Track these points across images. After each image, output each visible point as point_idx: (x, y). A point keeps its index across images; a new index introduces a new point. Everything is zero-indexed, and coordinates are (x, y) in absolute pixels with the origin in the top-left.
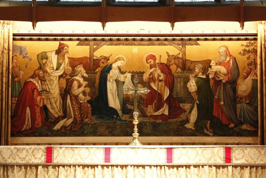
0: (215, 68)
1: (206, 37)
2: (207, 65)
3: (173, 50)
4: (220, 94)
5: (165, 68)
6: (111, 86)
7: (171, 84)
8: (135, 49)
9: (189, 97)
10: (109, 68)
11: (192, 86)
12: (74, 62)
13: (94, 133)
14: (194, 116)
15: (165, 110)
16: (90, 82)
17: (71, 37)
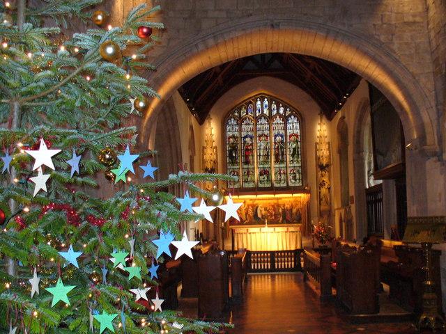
0: (286, 206)
1: (284, 198)
2: (284, 205)
3: (275, 201)
4: (288, 212)
5: (273, 206)
6: (259, 212)
7: (274, 210)
8: (265, 201)
9: (280, 214)
10: (257, 207)
11: (281, 211)
12: (248, 206)
13: (254, 224)
14: (281, 219)
15: (273, 217)
16: (253, 211)
17: (247, 199)
